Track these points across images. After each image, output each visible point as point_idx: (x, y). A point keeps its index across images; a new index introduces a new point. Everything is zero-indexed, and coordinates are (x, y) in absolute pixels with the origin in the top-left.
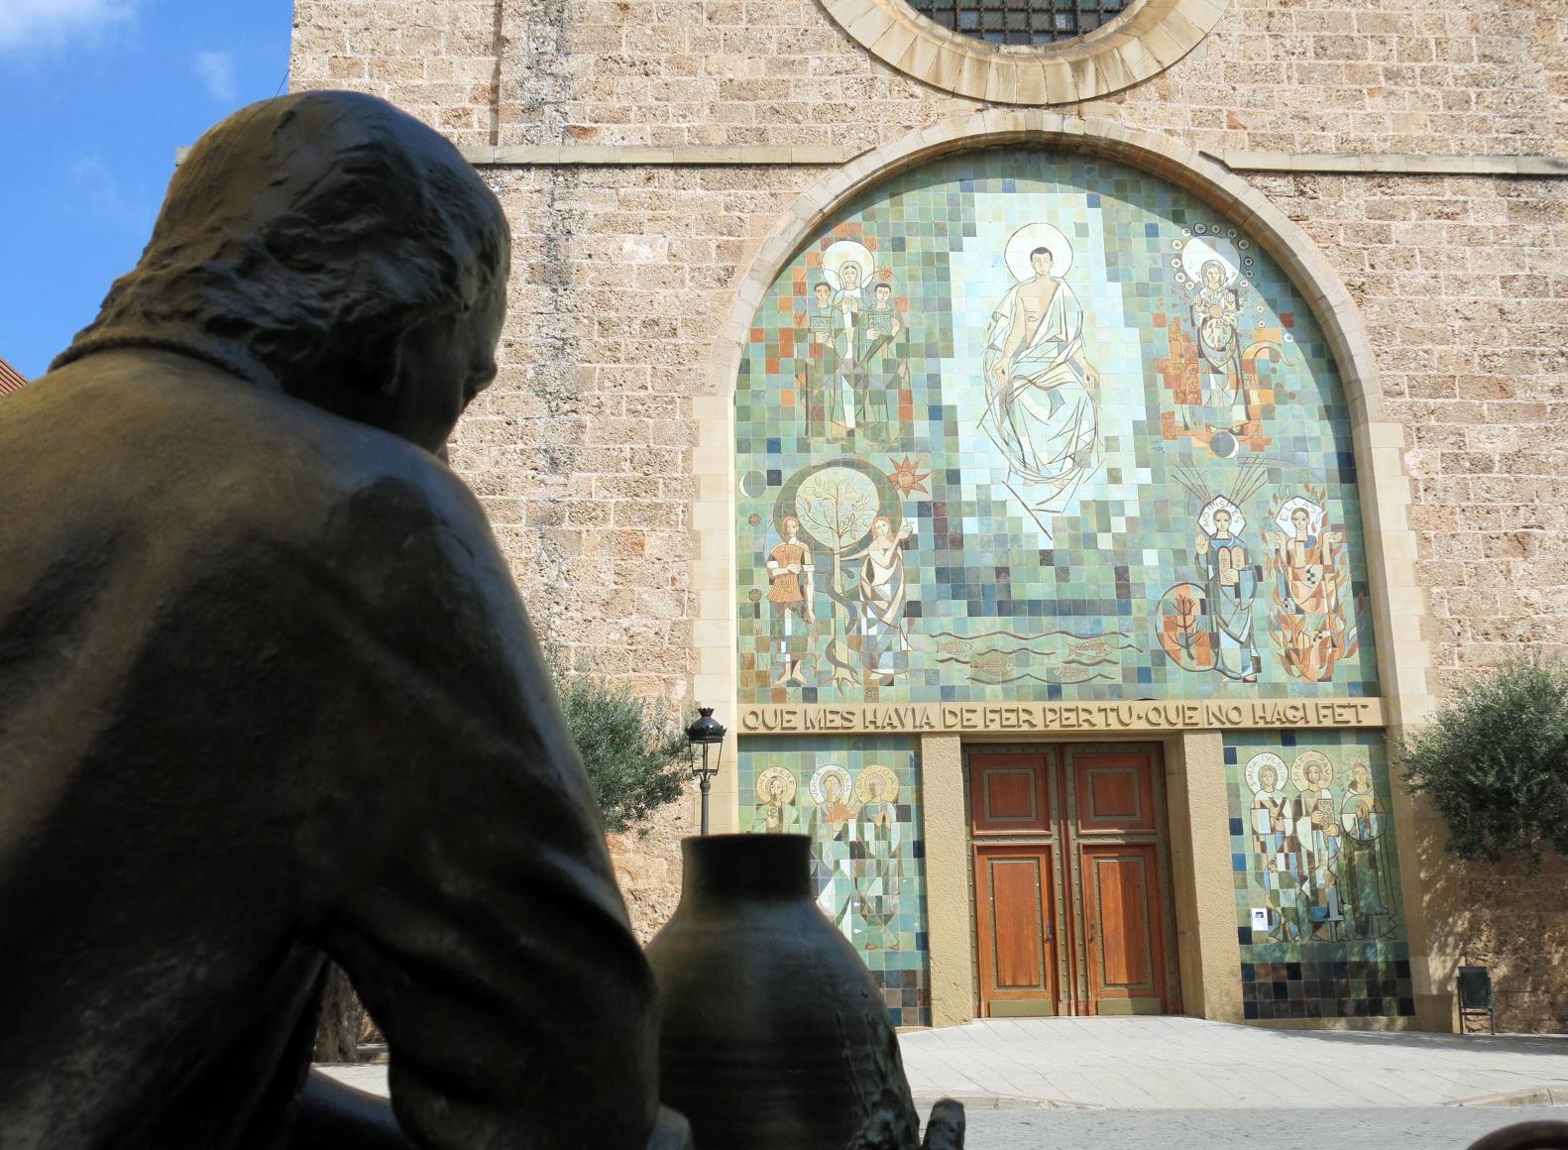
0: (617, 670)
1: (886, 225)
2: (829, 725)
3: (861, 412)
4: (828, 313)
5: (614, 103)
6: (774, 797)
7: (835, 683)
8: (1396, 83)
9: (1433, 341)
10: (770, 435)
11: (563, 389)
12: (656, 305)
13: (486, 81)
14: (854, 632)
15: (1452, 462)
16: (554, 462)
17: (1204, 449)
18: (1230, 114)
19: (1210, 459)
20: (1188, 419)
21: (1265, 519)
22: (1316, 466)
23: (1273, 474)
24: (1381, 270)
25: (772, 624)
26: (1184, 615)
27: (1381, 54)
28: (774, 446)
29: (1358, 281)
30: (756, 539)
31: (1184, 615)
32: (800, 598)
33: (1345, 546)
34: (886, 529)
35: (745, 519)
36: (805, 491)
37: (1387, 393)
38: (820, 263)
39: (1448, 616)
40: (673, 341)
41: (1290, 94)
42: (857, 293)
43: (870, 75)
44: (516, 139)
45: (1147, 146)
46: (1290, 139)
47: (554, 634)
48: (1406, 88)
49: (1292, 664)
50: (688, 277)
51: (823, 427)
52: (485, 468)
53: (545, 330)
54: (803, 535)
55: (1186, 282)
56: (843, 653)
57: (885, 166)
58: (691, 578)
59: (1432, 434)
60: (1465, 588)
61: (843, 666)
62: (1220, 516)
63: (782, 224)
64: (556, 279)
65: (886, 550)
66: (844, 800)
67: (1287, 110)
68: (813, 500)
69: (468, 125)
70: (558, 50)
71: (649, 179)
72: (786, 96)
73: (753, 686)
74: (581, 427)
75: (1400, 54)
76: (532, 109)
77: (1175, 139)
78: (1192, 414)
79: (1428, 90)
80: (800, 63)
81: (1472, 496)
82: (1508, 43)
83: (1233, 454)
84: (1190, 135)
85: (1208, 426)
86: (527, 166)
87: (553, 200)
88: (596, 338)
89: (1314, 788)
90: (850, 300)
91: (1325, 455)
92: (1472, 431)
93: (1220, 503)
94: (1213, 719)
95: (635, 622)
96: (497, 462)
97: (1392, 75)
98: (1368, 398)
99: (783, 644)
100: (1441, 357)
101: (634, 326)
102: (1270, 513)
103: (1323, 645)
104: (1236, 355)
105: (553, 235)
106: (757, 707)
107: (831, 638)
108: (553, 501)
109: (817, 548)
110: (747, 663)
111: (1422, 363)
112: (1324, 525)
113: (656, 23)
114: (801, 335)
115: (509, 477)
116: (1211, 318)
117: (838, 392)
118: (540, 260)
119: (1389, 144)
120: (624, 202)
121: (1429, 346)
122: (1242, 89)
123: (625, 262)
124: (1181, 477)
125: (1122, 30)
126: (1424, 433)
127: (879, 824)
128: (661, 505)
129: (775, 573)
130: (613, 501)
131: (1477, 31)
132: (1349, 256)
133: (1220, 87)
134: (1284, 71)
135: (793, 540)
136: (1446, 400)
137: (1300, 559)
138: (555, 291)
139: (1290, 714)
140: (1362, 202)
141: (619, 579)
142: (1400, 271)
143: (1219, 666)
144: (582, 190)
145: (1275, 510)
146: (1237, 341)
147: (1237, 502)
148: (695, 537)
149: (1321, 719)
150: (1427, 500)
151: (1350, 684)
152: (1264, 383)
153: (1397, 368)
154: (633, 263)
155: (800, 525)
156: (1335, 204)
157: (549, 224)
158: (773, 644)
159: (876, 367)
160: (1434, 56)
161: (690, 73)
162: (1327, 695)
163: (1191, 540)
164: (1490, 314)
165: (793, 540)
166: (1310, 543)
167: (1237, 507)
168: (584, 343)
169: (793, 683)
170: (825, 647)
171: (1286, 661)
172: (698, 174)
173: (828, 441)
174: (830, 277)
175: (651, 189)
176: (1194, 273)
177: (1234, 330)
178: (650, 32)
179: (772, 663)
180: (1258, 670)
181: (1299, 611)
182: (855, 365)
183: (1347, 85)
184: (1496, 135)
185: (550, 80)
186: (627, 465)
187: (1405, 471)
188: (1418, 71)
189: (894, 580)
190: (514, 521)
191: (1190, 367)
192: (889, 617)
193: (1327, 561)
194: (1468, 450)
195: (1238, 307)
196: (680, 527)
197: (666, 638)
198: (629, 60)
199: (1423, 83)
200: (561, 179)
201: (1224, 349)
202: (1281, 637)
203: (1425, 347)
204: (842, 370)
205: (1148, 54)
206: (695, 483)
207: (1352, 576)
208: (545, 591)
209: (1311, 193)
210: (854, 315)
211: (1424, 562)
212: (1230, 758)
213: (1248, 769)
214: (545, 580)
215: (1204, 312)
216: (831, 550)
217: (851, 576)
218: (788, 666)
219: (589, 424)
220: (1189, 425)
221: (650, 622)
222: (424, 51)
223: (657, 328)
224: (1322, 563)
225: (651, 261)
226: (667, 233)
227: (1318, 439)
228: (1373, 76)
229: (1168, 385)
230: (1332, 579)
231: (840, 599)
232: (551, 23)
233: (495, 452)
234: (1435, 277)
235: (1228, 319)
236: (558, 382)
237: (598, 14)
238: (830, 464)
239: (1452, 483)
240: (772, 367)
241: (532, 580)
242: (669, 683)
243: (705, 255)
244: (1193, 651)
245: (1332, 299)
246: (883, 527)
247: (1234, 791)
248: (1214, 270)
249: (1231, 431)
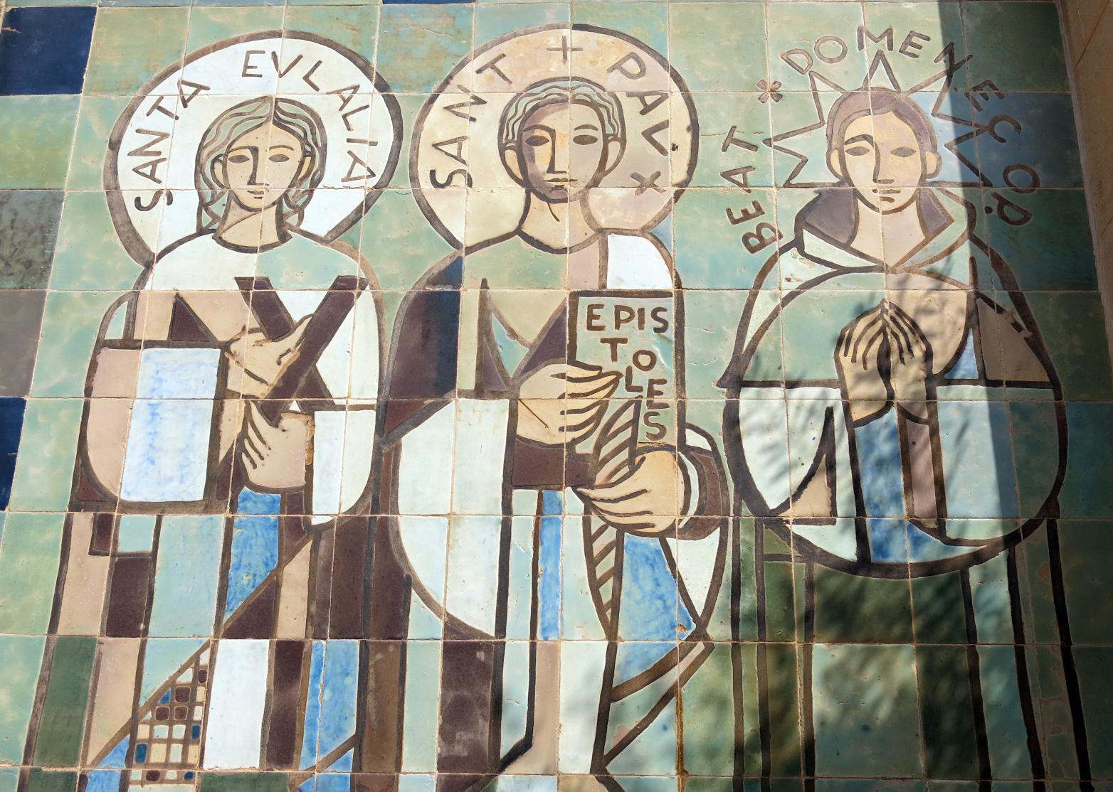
213: (139, 119)
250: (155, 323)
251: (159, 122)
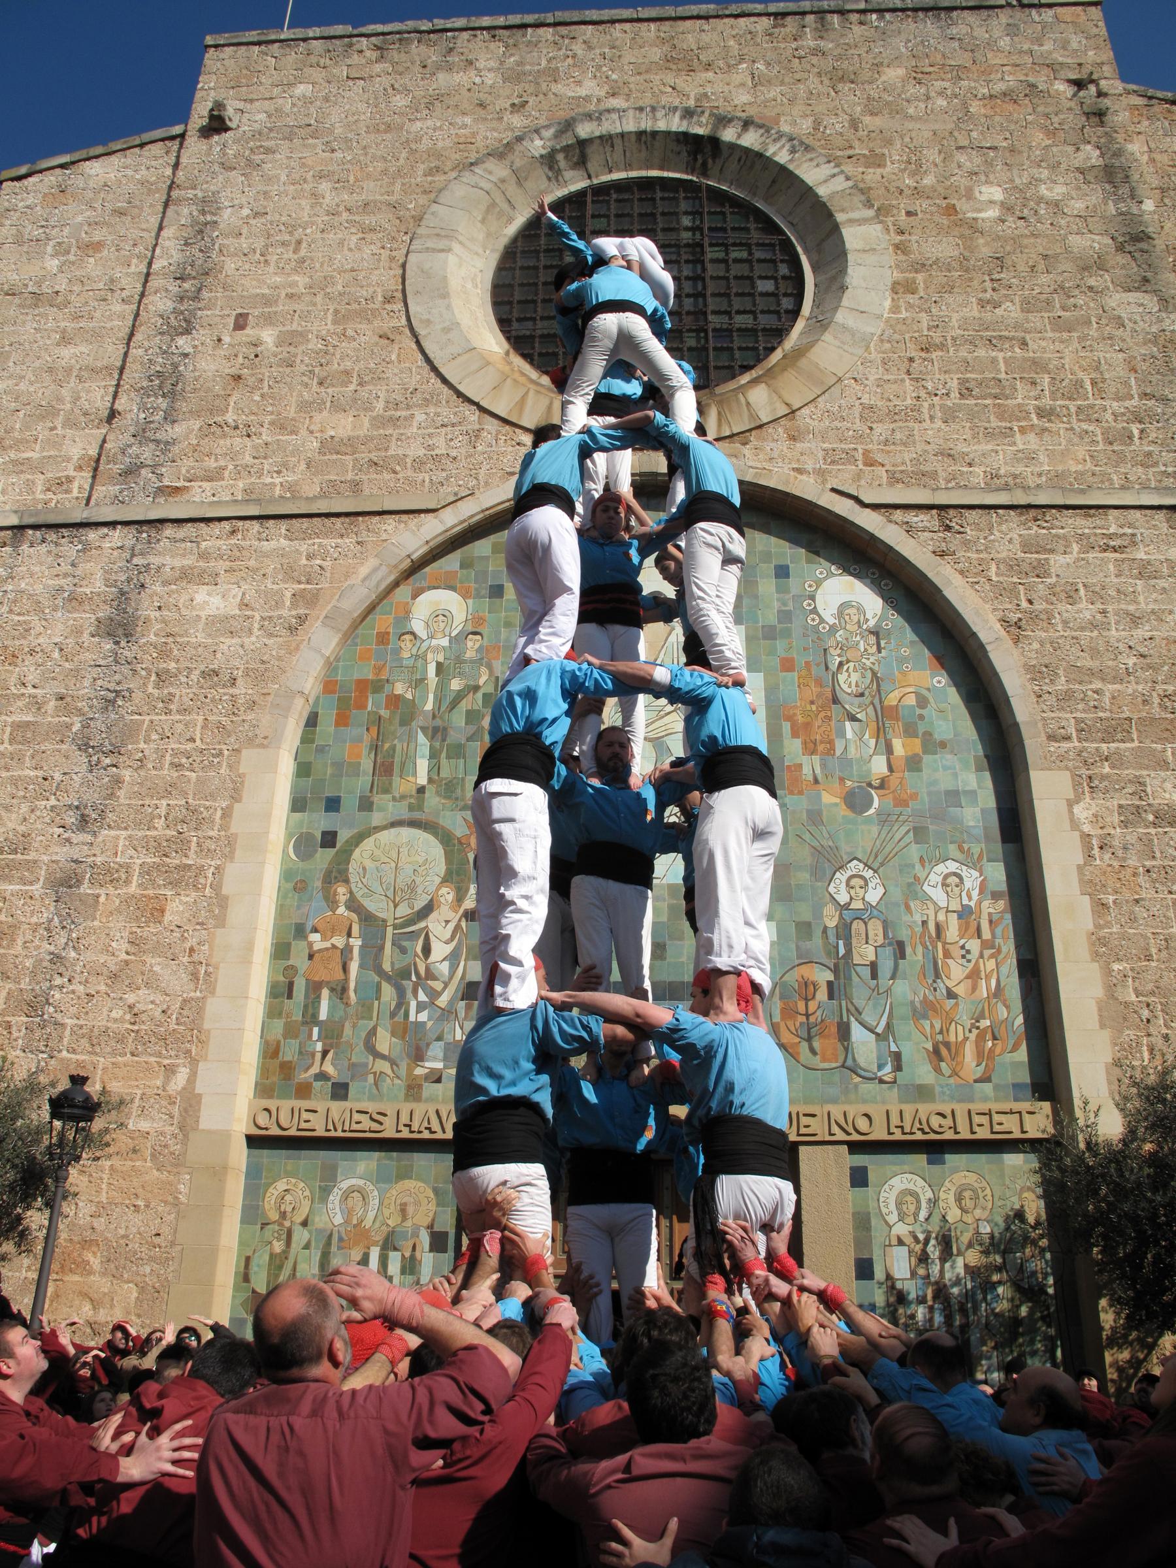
0: (114, 1053)
1: (485, 573)
2: (355, 1127)
3: (435, 768)
4: (411, 662)
5: (211, 463)
6: (283, 1215)
7: (371, 1078)
8: (1050, 421)
9: (1103, 680)
10: (329, 793)
11: (107, 743)
12: (219, 655)
13: (93, 452)
14: (400, 1018)
15: (1132, 815)
16: (84, 820)
17: (836, 805)
18: (866, 453)
19: (844, 817)
20: (818, 771)
21: (909, 885)
22: (971, 824)
23: (920, 833)
24: (1039, 606)
25: (306, 1006)
26: (807, 1000)
27: (1032, 394)
28: (333, 804)
29: (1014, 617)
30: (299, 907)
31: (807, 1000)
32: (341, 976)
33: (1008, 916)
34: (450, 897)
35: (290, 886)
36: (362, 855)
37: (1051, 737)
38: (408, 612)
39: (1133, 998)
40: (231, 691)
41: (932, 431)
42: (445, 642)
43: (477, 427)
44: (108, 501)
45: (772, 484)
46: (934, 475)
47: (51, 1009)
48: (1062, 425)
49: (942, 1061)
50: (256, 626)
51: (390, 784)
52: (11, 825)
53: (99, 682)
54: (353, 905)
55: (819, 624)
56: (385, 1042)
57: (483, 511)
58: (211, 948)
59: (1106, 783)
60: (1154, 964)
61: (383, 1057)
62: (856, 882)
63: (364, 571)
64: (120, 631)
65: (447, 922)
66: (368, 1223)
67: (928, 447)
68: (369, 864)
69: (67, 491)
70: (166, 418)
71: (234, 531)
72: (386, 450)
73: (275, 1079)
74: (118, 781)
75: (1052, 393)
76: (130, 472)
77: (804, 477)
78: (824, 766)
79: (1085, 426)
80: (406, 419)
81: (1158, 855)
82: (1171, 382)
83: (872, 811)
84: (821, 473)
85: (842, 780)
86: (112, 524)
87: (133, 555)
88: (150, 690)
89: (968, 1219)
90: (437, 649)
91: (982, 810)
92: (1154, 780)
93: (855, 867)
94: (835, 1129)
95: (140, 997)
96: (25, 819)
97: (1042, 413)
98: (1028, 743)
99: (316, 1030)
100: (1114, 698)
101: (192, 676)
102: (916, 878)
103: (981, 1038)
104: (876, 701)
105: (126, 589)
106: (272, 1104)
107: (372, 1024)
108: (76, 861)
109: (367, 918)
110: (270, 1051)
111: (1092, 704)
112: (981, 892)
113: (266, 389)
114: (377, 686)
115: (33, 835)
116: (848, 661)
117: (412, 746)
118: (108, 613)
119: (1044, 479)
120: (204, 556)
121: (1097, 685)
122: (879, 428)
123: (194, 613)
124: (807, 836)
125: (755, 381)
126: (1096, 782)
127: (407, 1254)
128: (190, 866)
129: (316, 947)
130: (139, 862)
131: (1136, 372)
132: (1002, 591)
133: (855, 427)
134: (925, 411)
135: (341, 910)
136: (1122, 745)
137: (952, 932)
138: (117, 643)
139: (935, 1122)
140: (1016, 536)
141: (132, 949)
142: (1063, 607)
143: (849, 1062)
144: (165, 543)
145: (922, 875)
146: (878, 686)
147: (875, 866)
148: (223, 902)
149: (976, 1129)
150: (1102, 860)
151: (1015, 1086)
152: (910, 731)
153: (1063, 709)
154: (203, 614)
155: (351, 892)
156: (985, 538)
157: (123, 578)
158: (305, 1029)
159: (458, 719)
160: (1090, 395)
161: (293, 432)
162: (985, 1099)
163: (818, 913)
164: (1169, 651)
165: (341, 910)
166: (965, 913)
167: (875, 871)
168: (138, 696)
169: (322, 1076)
170: (363, 1035)
171: (933, 1057)
172: (283, 525)
173: (394, 799)
174: (418, 626)
175: (232, 542)
176: (828, 613)
177: (874, 674)
178: (257, 398)
179: (300, 1053)
180: (898, 1068)
181: (951, 995)
182: (434, 717)
183: (995, 423)
184: (1163, 469)
185: (152, 446)
186: (160, 823)
187: (1075, 824)
188: (1073, 409)
189: (453, 958)
190: (31, 883)
191: (822, 714)
192: (443, 1000)
193: (986, 934)
194: (1151, 801)
195: (879, 650)
196: (208, 891)
197: (174, 1017)
198: (233, 424)
199: (1080, 420)
200: (145, 535)
201: (862, 695)
202: (928, 1028)
203: (1093, 686)
204: (420, 721)
205: (776, 398)
206: (231, 842)
207: (1018, 954)
208: (51, 961)
209: (957, 527)
210: (439, 666)
211: (1101, 933)
212: (859, 1178)
213: (883, 1194)
214: (52, 948)
215: (839, 655)
216: (384, 921)
217: (404, 951)
218: (318, 1056)
219: (127, 779)
220: (820, 778)
221: (159, 998)
222: (41, 430)
223: (216, 679)
224: (979, 937)
225: (222, 612)
226: (242, 583)
227: (972, 794)
228: (1024, 414)
229: (795, 734)
230: (992, 956)
231: (388, 978)
232: (164, 396)
233: (24, 808)
234: (1104, 612)
235: (868, 663)
236: (104, 735)
237: (210, 384)
238: (393, 824)
239: (1132, 838)
240: (342, 720)
241: (39, 947)
242: (170, 1070)
243: (278, 604)
244: (816, 1044)
245: (983, 636)
246: (447, 895)
247: (863, 1222)
248: (852, 611)
249: (870, 785)
250: (894, 1241)
251: (886, 1195)
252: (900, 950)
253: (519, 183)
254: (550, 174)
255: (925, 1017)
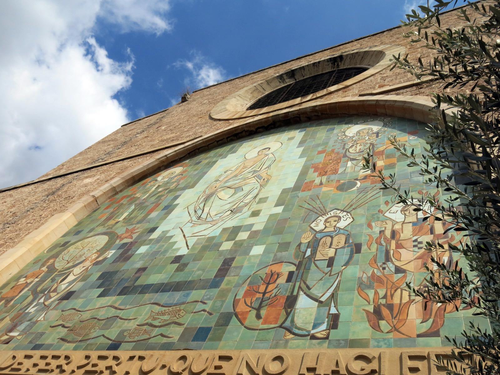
49: (382, 319)
83: (355, 188)
171: (373, 317)
244: (263, 312)
252: (358, 248)
253: (268, 84)
254: (280, 81)
255: (370, 287)
